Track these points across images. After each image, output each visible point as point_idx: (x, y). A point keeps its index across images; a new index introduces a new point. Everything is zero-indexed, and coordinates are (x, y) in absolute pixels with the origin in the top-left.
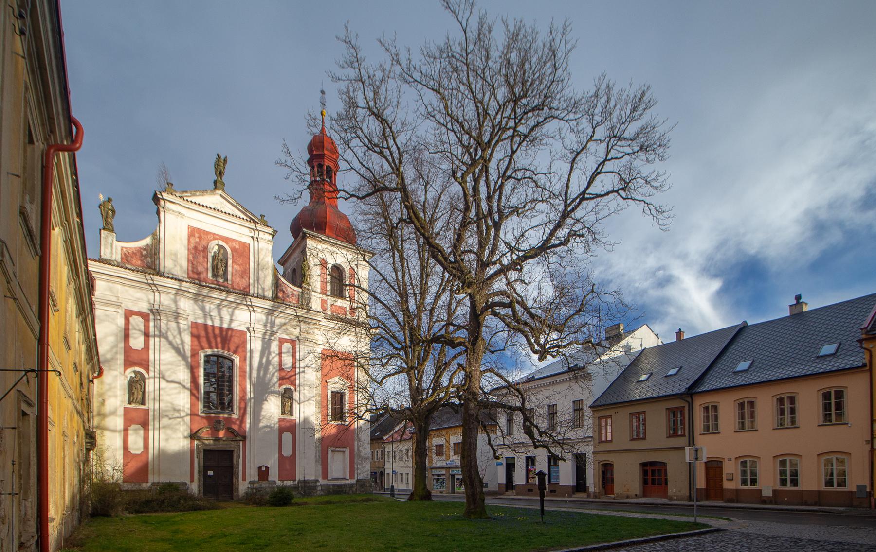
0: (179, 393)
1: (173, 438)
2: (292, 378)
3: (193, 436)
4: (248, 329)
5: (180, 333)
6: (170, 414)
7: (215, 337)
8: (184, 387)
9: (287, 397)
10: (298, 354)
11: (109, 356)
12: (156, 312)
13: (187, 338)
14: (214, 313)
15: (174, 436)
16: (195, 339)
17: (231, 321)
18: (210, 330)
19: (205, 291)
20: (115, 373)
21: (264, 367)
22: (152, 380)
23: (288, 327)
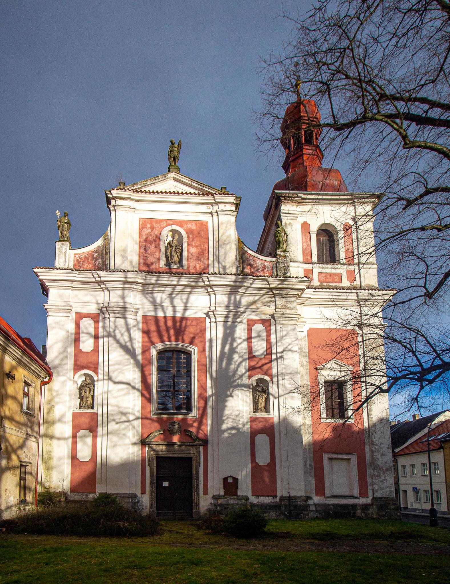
0: (128, 394)
1: (121, 447)
2: (266, 367)
3: (143, 442)
4: (207, 314)
5: (128, 330)
6: (117, 417)
7: (168, 329)
8: (134, 388)
9: (261, 391)
10: (273, 337)
11: (57, 362)
12: (103, 310)
13: (138, 336)
14: (167, 303)
15: (120, 442)
16: (145, 335)
17: (185, 309)
18: (162, 323)
19: (153, 279)
20: (62, 378)
21: (227, 356)
22: (100, 383)
23: (259, 305)
